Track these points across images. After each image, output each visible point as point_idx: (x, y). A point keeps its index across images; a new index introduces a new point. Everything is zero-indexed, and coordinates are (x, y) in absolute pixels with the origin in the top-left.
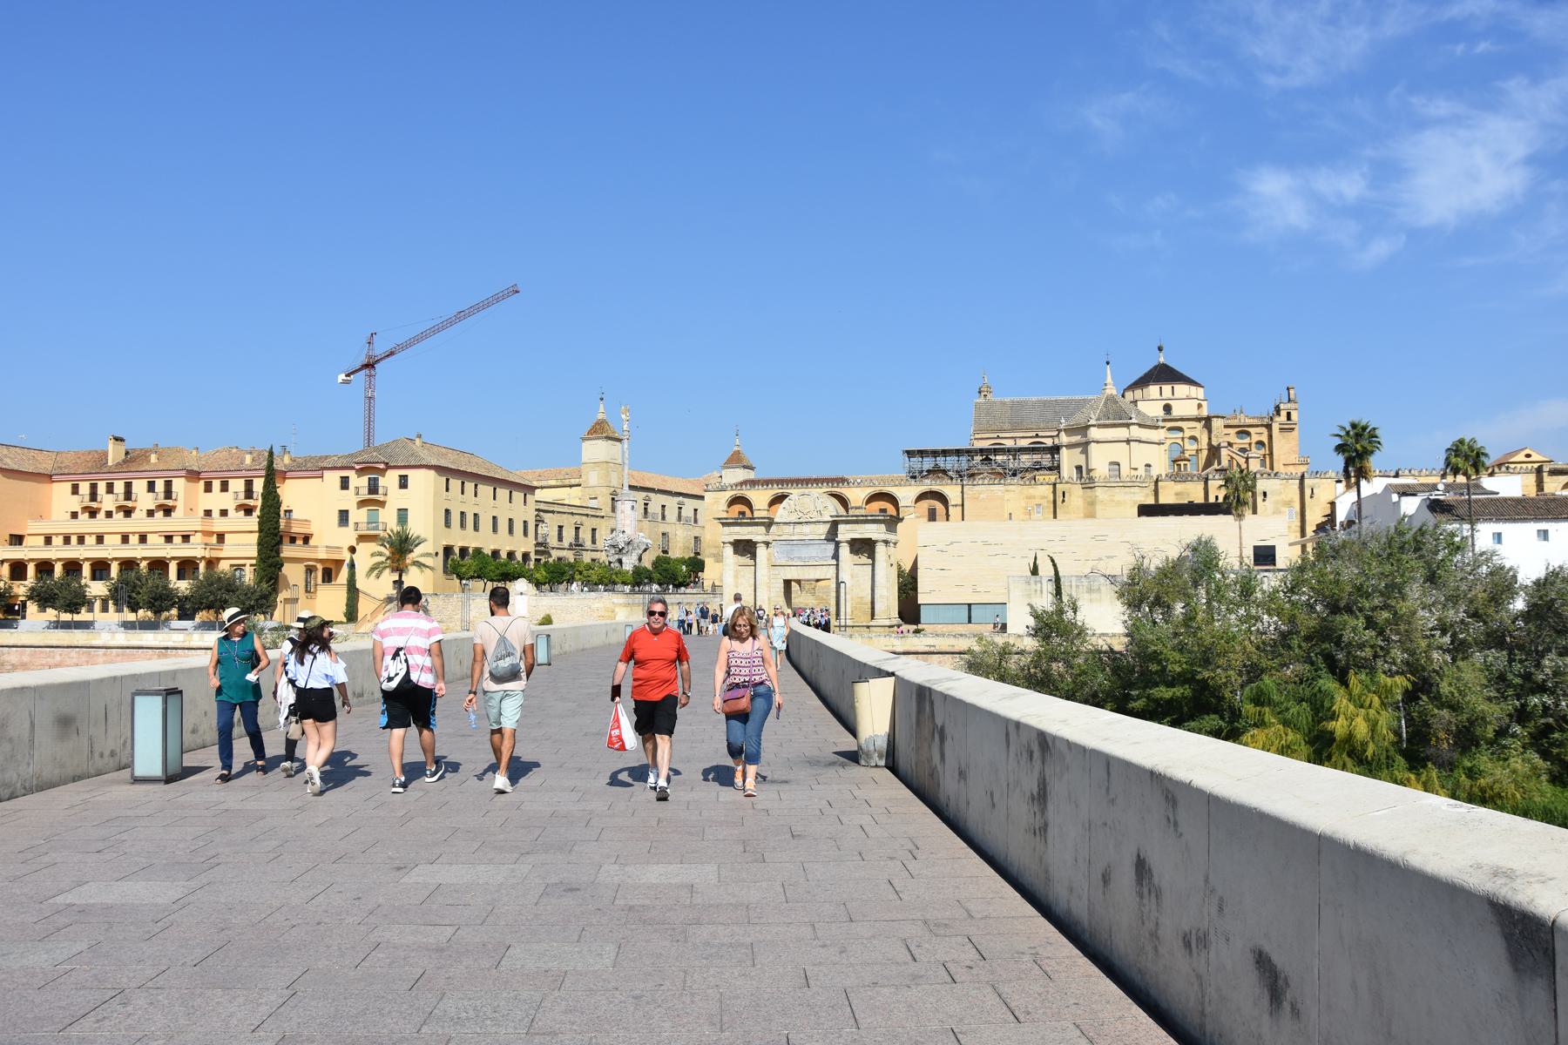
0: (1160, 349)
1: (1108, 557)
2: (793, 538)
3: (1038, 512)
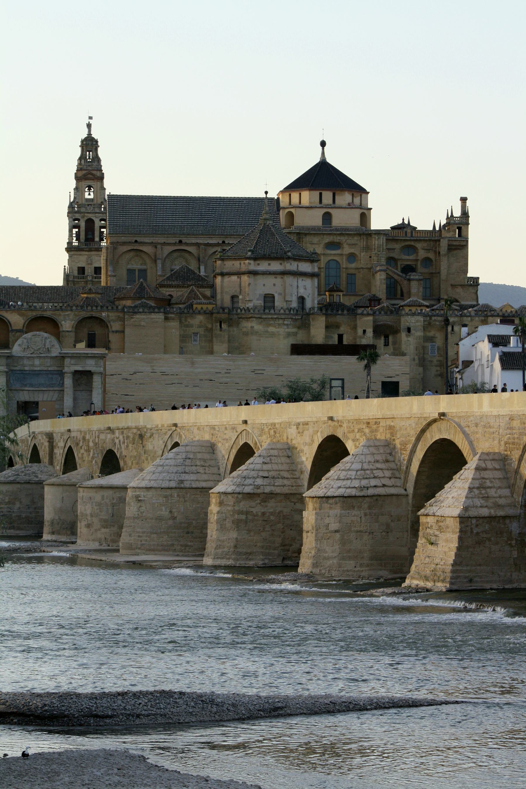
0: (323, 144)
2: (26, 368)
3: (195, 340)
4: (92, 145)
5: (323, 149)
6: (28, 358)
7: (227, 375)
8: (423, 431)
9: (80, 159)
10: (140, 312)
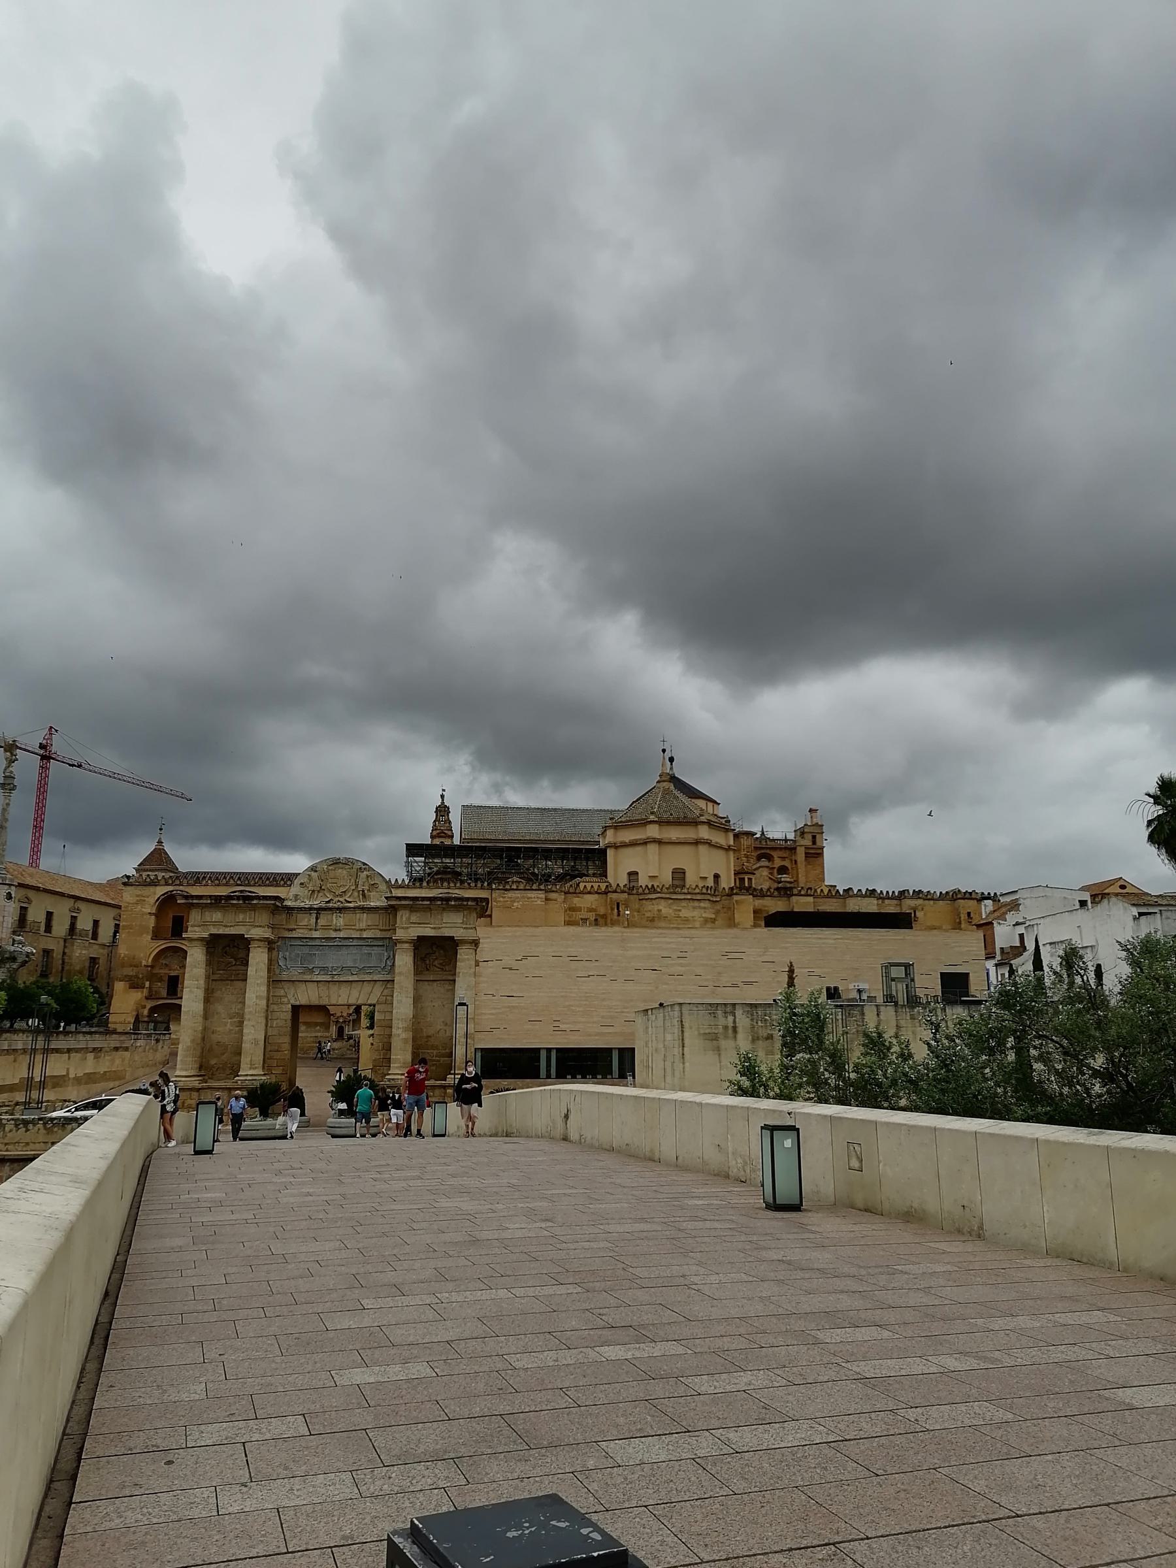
1: (746, 983)
2: (316, 934)
4: (445, 810)
5: (672, 764)
6: (319, 910)
7: (681, 961)
9: (435, 821)
10: (513, 889)
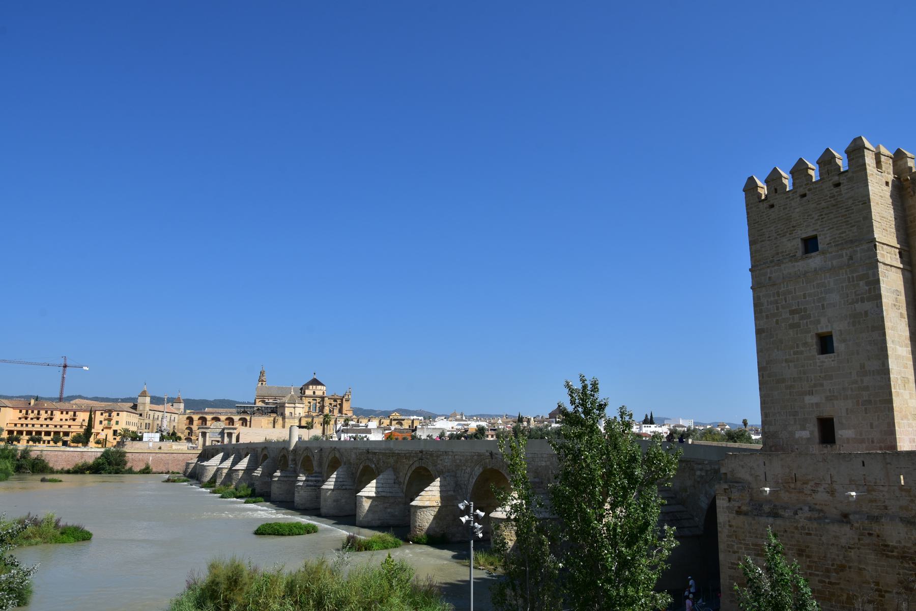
8: (262, 452)
